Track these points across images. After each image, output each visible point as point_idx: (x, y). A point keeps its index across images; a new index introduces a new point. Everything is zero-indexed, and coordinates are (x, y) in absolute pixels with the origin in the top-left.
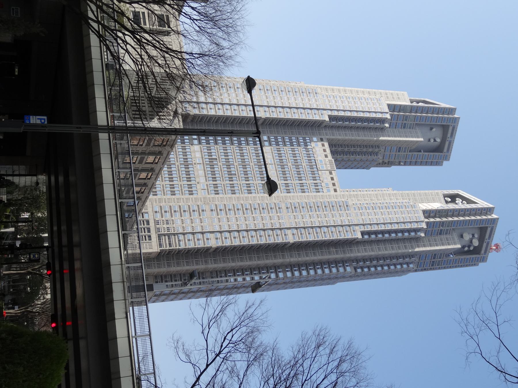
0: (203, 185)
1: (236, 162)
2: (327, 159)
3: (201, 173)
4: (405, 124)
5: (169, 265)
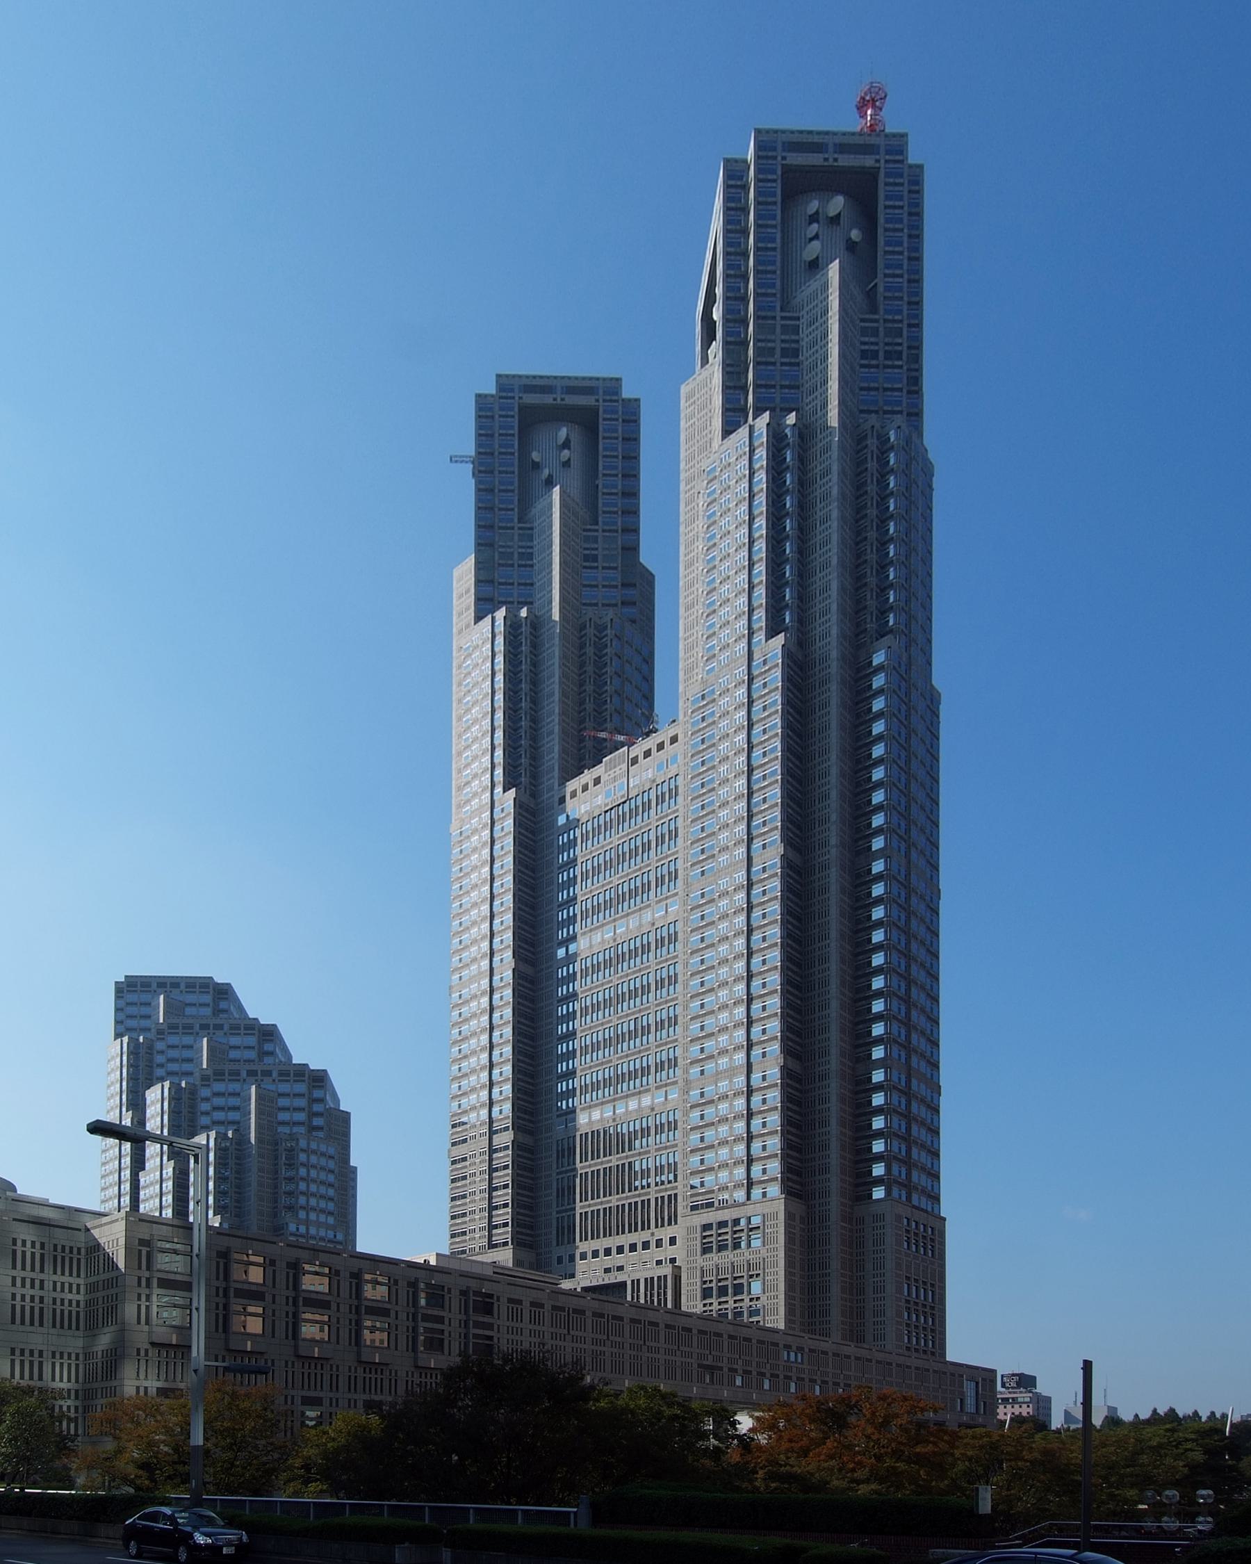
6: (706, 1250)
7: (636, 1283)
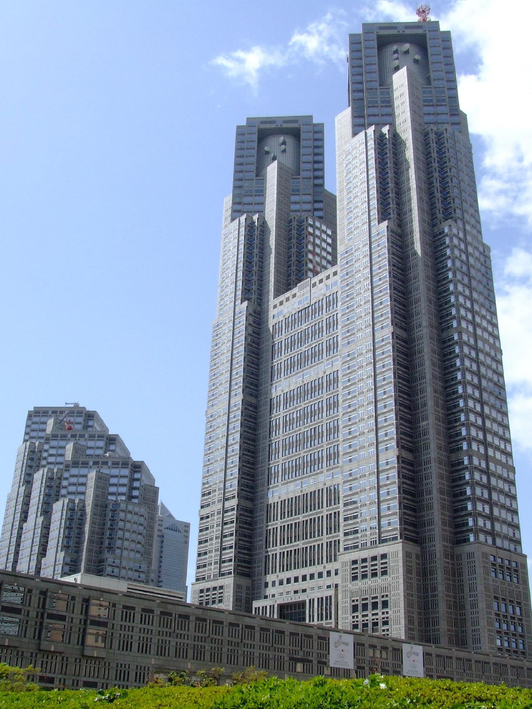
0: (328, 476)
1: (300, 429)
2: (298, 294)
3: (311, 480)
4: (257, 191)
5: (431, 522)
6: (355, 578)
7: (311, 601)
